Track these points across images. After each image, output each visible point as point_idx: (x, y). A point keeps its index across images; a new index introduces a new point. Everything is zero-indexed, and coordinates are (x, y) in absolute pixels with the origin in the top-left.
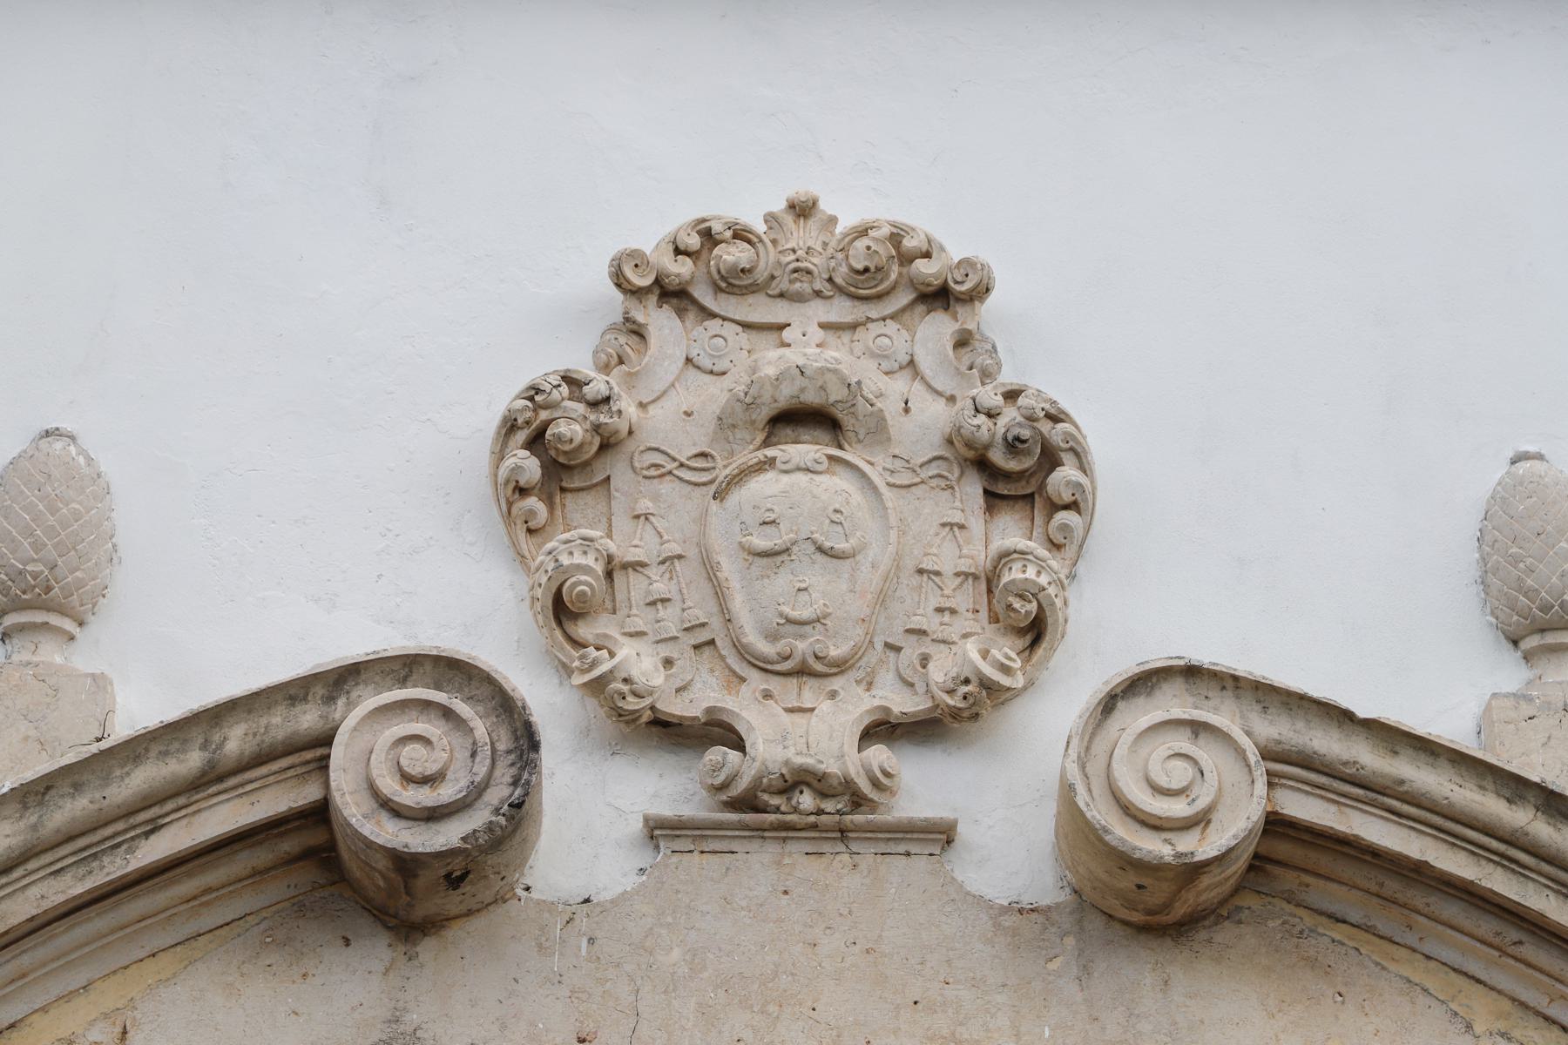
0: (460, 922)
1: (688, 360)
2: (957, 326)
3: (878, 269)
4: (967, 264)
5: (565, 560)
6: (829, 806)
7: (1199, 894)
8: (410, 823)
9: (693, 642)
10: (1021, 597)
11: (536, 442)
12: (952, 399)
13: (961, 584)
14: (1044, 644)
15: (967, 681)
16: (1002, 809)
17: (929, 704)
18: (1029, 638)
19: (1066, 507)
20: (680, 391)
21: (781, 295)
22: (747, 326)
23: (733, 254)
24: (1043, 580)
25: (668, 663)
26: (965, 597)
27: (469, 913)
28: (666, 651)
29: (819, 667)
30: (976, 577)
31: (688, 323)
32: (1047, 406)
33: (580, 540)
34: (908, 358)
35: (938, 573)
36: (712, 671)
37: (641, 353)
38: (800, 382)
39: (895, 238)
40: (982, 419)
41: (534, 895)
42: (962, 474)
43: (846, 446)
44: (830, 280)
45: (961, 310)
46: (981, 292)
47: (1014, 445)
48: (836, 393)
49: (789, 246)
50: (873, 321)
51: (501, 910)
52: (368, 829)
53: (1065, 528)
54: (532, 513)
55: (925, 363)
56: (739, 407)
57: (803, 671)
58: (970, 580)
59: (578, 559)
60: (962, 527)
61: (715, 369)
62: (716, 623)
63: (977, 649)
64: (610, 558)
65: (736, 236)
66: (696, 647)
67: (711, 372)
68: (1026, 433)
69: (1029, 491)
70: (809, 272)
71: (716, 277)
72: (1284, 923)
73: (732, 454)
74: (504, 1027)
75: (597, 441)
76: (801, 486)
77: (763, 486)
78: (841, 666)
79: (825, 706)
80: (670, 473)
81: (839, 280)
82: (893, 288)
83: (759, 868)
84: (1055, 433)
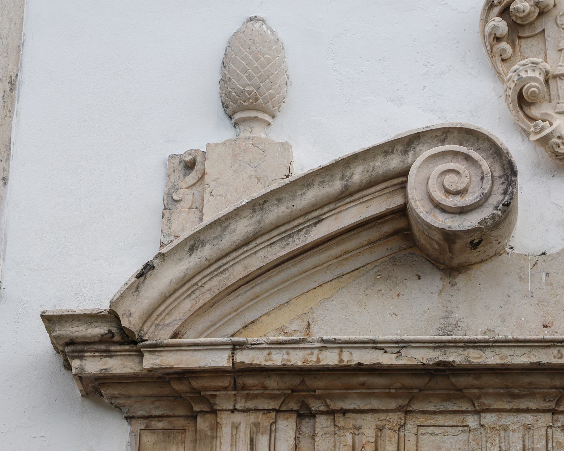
0: (475, 267)
5: (523, 75)
27: (482, 261)
33: (530, 64)
41: (516, 251)
51: (498, 259)
59: (530, 74)
64: (547, 73)
74: (504, 320)
75: (537, 10)
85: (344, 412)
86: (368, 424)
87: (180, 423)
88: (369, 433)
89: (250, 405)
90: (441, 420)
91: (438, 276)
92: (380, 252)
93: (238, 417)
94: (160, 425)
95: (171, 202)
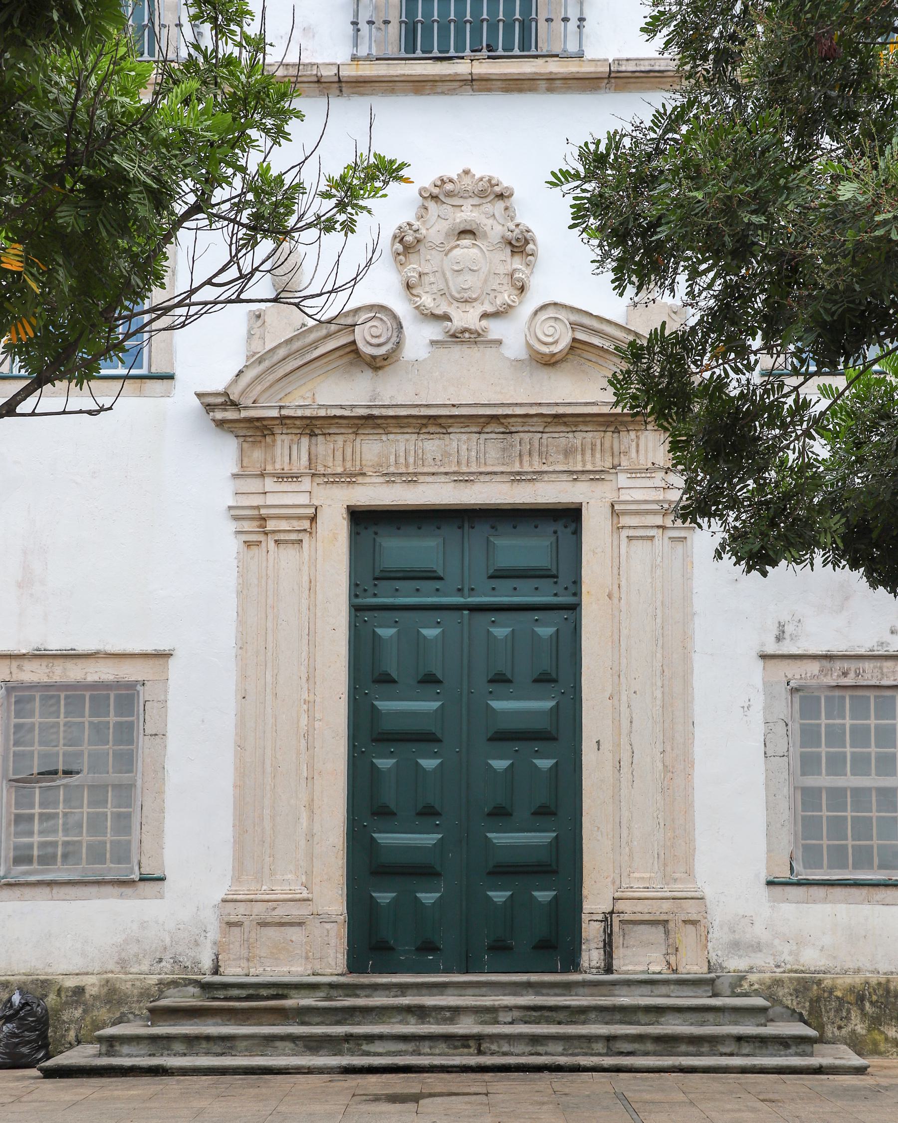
4: (507, 188)
6: (472, 336)
11: (401, 241)
16: (512, 335)
20: (436, 228)
22: (453, 206)
23: (449, 187)
25: (434, 299)
26: (505, 280)
28: (434, 296)
33: (413, 268)
37: (427, 214)
39: (490, 181)
45: (506, 200)
46: (511, 195)
47: (518, 240)
48: (474, 226)
53: (530, 261)
55: (497, 215)
57: (466, 301)
59: (412, 274)
62: (446, 289)
63: (506, 296)
68: (520, 237)
76: (466, 251)
77: (457, 252)
78: (475, 300)
79: (472, 310)
83: (457, 352)
84: (528, 235)
85: (330, 434)
86: (340, 439)
87: (259, 439)
88: (340, 443)
89: (289, 431)
90: (371, 437)
91: (370, 371)
92: (345, 359)
93: (284, 437)
94: (250, 439)
95: (250, 335)
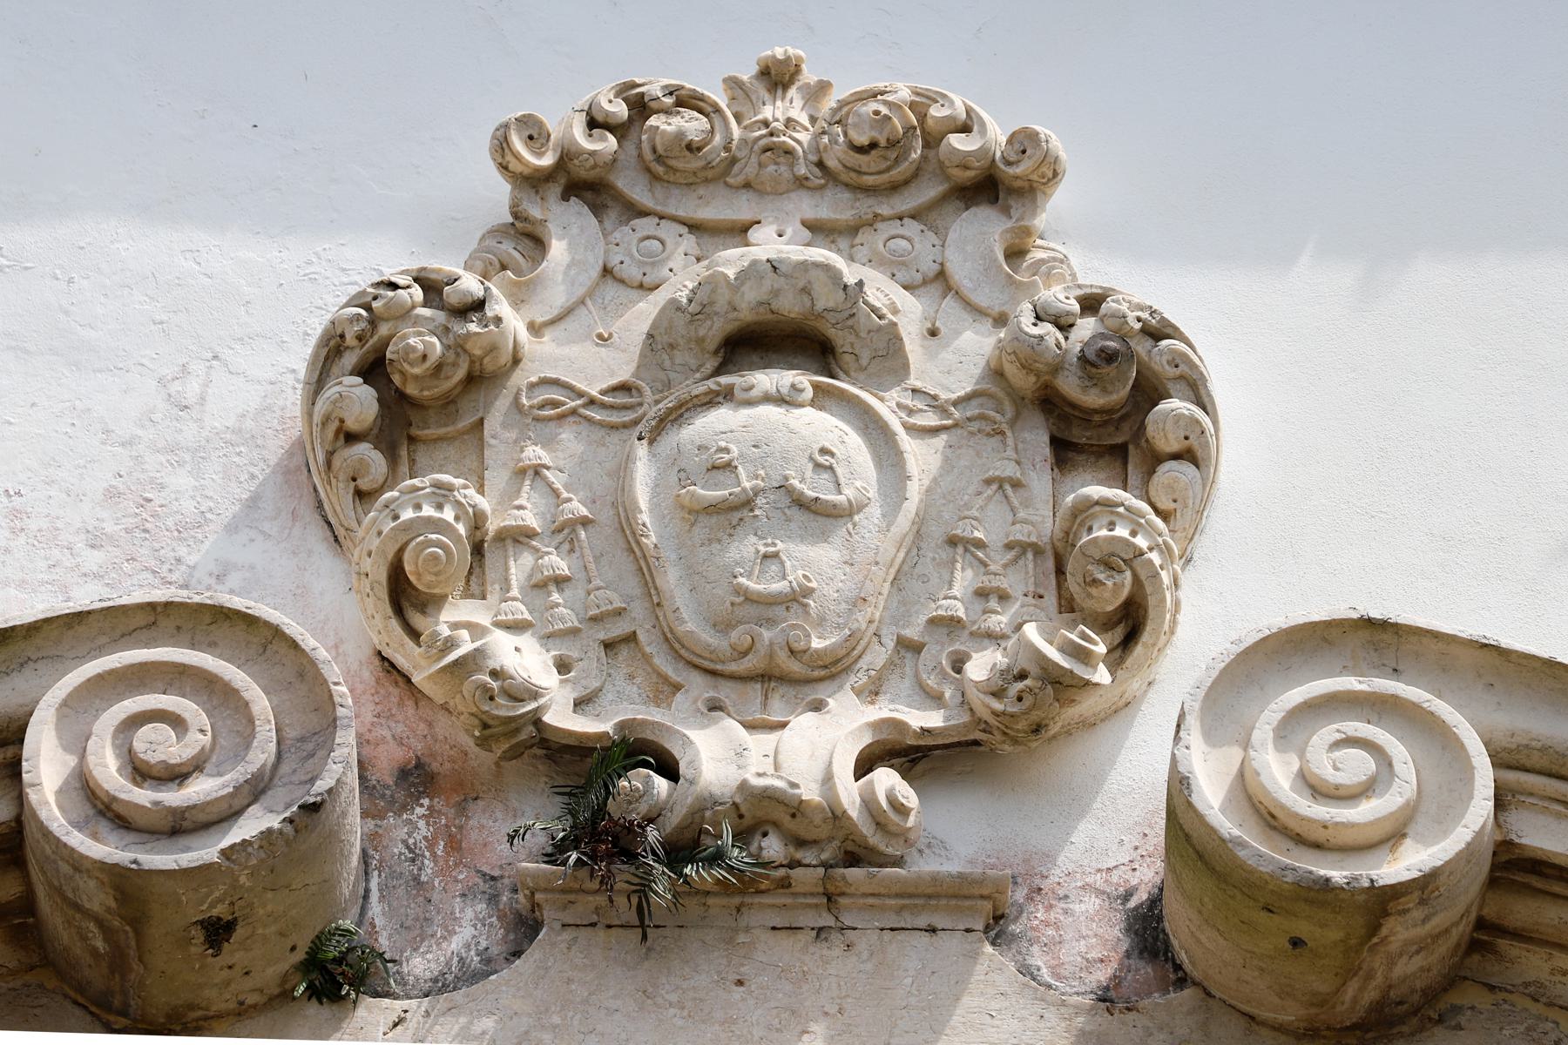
1: (607, 271)
2: (1009, 224)
3: (892, 144)
6: (808, 856)
7: (1391, 962)
8: (146, 837)
9: (602, 636)
10: (1109, 566)
11: (374, 369)
12: (1001, 320)
13: (1015, 560)
14: (1146, 637)
15: (1022, 676)
17: (966, 718)
18: (1118, 633)
19: (1176, 456)
21: (747, 185)
22: (694, 227)
24: (1141, 542)
29: (795, 667)
30: (1038, 551)
31: (608, 224)
32: (1145, 315)
33: (434, 501)
34: (936, 267)
35: (980, 544)
36: (631, 677)
38: (771, 280)
39: (919, 106)
40: (1047, 328)
42: (1017, 416)
43: (841, 374)
44: (820, 164)
48: (826, 299)
49: (760, 117)
50: (885, 219)
52: (79, 841)
54: (363, 462)
55: (960, 272)
56: (680, 320)
57: (768, 677)
58: (1030, 556)
60: (1016, 485)
61: (647, 280)
62: (638, 610)
64: (477, 521)
65: (680, 103)
66: (608, 646)
67: (641, 286)
69: (1119, 440)
70: (789, 152)
71: (649, 156)
72: (1528, 1029)
73: (668, 385)
76: (776, 423)
77: (716, 425)
80: (574, 412)
81: (831, 163)
82: (916, 174)
